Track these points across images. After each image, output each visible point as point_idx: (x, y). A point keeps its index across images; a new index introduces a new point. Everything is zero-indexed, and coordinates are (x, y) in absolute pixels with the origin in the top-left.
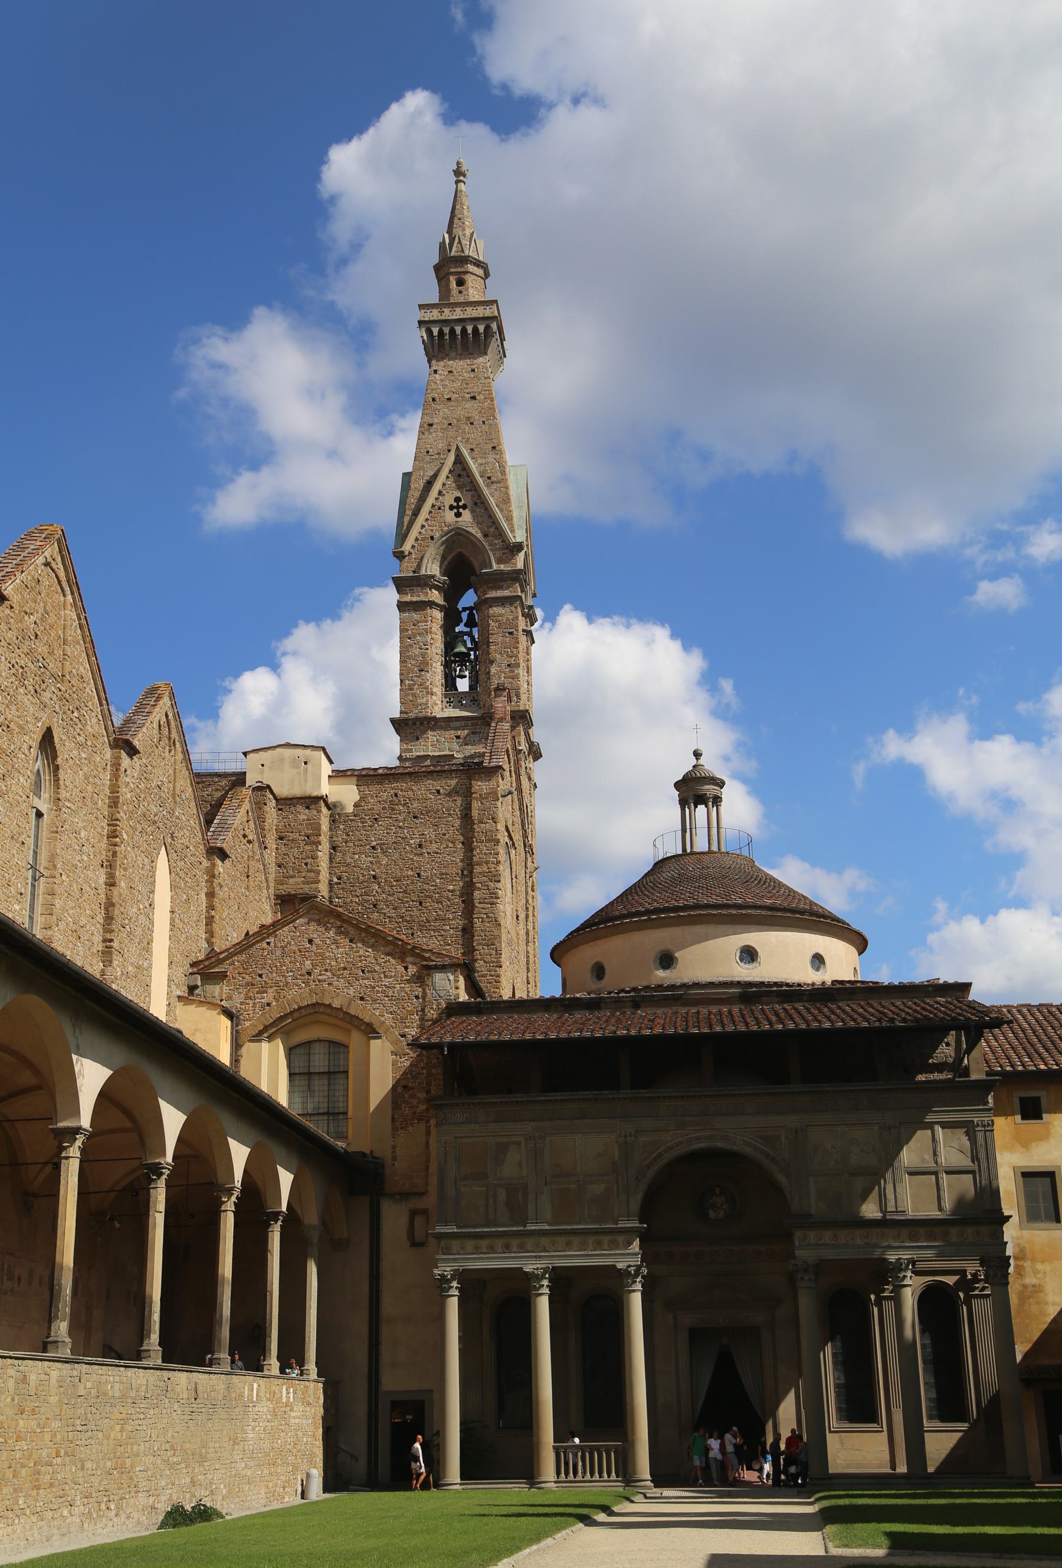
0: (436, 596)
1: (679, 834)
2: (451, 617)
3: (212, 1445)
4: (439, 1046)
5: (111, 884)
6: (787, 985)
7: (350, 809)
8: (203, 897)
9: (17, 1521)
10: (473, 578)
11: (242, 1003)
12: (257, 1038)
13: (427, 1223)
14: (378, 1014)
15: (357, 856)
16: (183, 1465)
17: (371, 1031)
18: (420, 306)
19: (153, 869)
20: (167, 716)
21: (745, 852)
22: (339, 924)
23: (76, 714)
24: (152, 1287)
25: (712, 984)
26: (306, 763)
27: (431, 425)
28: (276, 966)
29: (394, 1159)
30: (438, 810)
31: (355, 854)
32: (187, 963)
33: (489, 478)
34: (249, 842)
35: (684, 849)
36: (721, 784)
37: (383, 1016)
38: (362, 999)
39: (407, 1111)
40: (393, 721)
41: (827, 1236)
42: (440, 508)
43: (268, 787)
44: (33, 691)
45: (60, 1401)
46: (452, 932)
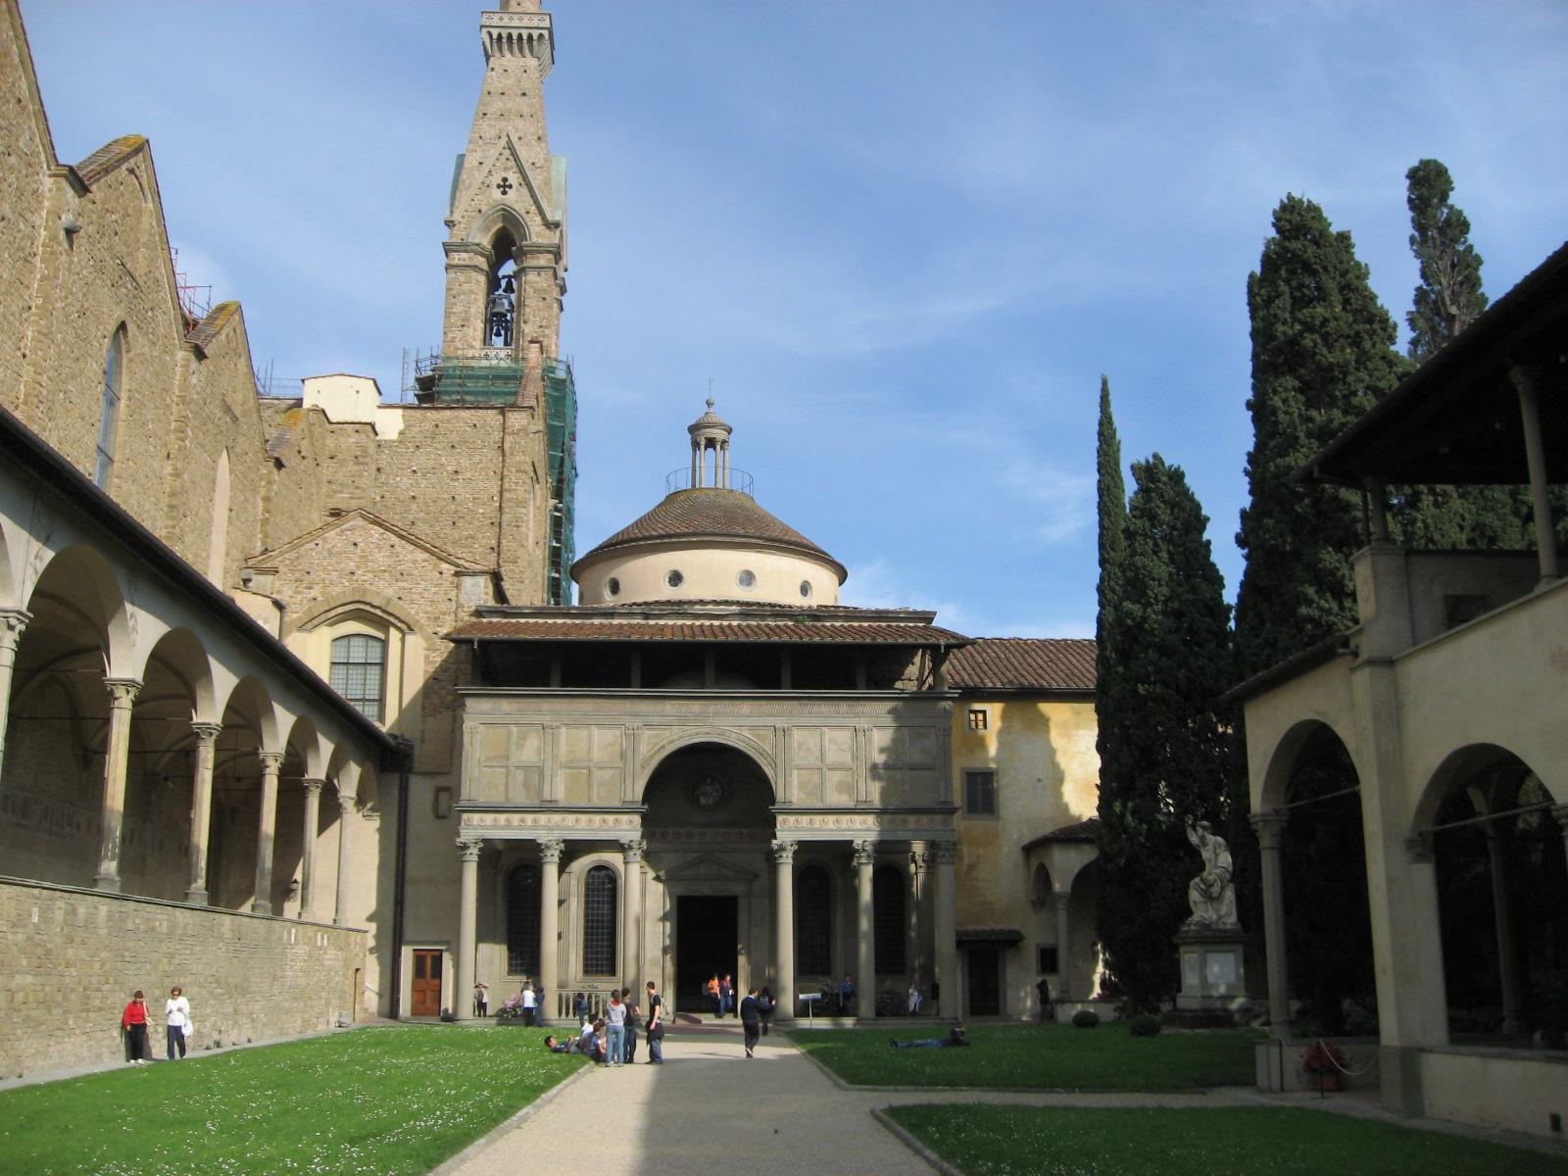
0: (482, 262)
1: (690, 470)
2: (493, 284)
3: (253, 979)
4: (470, 642)
6: (780, 606)
7: (394, 436)
8: (259, 499)
9: (67, 1040)
10: (514, 248)
11: (291, 597)
12: (301, 628)
13: (450, 798)
14: (413, 613)
15: (398, 479)
16: (227, 996)
19: (214, 469)
20: (235, 330)
21: (746, 491)
22: (382, 531)
23: (150, 314)
24: (199, 836)
25: (714, 602)
26: (358, 392)
27: (485, 114)
28: (323, 566)
29: (423, 741)
30: (473, 442)
31: (397, 476)
32: (241, 557)
33: (533, 164)
34: (304, 458)
35: (694, 485)
36: (730, 431)
37: (418, 614)
38: (400, 598)
41: (805, 819)
42: (488, 186)
43: (323, 411)
44: (110, 285)
45: (109, 934)
46: (480, 550)
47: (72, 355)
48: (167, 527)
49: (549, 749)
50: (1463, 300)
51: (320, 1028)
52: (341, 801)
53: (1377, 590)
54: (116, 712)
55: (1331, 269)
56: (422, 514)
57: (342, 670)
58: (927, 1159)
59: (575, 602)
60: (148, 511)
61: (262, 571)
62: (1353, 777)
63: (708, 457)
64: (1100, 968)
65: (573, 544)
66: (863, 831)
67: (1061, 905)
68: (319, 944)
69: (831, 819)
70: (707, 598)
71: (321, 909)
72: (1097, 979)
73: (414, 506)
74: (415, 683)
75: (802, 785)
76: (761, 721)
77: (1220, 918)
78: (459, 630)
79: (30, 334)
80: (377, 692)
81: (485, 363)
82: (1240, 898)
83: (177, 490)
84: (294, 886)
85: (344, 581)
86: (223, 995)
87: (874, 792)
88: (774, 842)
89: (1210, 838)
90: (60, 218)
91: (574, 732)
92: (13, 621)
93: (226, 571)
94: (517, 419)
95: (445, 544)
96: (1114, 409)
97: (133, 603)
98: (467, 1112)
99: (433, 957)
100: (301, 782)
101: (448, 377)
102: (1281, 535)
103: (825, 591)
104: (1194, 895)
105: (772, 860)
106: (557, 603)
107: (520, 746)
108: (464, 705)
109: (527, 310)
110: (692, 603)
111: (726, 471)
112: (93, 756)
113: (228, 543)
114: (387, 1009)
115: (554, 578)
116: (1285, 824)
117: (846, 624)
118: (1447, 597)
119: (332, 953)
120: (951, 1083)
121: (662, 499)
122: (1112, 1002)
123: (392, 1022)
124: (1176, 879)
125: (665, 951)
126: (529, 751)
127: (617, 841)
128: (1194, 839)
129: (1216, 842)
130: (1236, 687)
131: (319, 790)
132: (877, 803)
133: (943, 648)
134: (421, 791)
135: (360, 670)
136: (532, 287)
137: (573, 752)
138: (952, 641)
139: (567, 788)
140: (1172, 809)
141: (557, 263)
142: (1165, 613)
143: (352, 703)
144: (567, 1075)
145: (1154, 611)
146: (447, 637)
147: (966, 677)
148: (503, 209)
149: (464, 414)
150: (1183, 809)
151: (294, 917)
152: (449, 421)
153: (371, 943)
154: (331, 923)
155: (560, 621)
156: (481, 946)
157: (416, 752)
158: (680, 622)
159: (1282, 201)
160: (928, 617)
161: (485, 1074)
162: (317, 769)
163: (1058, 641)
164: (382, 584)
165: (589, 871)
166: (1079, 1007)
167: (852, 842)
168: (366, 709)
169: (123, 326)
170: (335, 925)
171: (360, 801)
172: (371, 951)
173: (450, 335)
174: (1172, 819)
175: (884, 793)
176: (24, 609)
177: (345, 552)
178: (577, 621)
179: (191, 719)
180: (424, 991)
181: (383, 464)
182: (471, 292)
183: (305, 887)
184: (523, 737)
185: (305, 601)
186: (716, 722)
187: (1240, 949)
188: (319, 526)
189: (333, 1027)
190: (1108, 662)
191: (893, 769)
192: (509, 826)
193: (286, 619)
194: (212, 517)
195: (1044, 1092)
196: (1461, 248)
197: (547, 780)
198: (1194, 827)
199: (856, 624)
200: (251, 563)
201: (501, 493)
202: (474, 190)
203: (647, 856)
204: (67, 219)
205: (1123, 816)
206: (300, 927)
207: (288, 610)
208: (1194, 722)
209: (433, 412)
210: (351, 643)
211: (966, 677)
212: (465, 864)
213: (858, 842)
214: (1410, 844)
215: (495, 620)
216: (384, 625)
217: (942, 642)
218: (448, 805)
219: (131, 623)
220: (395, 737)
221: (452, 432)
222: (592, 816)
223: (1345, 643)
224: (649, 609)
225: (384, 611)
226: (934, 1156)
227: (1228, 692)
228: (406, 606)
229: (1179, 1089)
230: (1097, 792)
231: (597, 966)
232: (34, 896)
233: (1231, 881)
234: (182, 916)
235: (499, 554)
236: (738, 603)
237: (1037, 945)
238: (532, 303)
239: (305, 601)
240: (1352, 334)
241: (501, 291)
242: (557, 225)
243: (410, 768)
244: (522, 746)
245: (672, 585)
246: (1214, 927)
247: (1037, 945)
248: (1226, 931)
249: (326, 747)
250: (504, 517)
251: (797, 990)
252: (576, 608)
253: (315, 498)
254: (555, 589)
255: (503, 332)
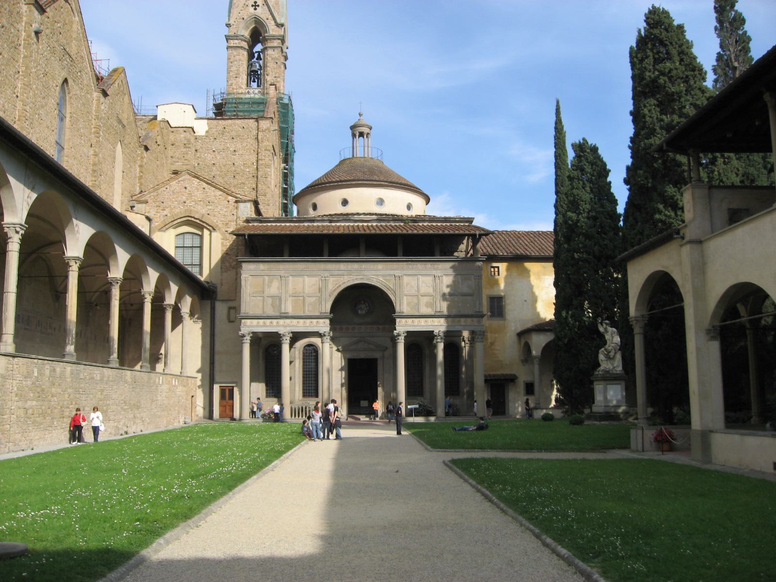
0: (245, 45)
1: (351, 149)
2: (251, 56)
3: (142, 401)
4: (244, 235)
6: (397, 215)
7: (203, 133)
9: (54, 432)
10: (261, 37)
11: (155, 215)
12: (160, 230)
13: (236, 312)
17: (212, 229)
19: (114, 152)
22: (198, 181)
23: (79, 74)
25: (364, 214)
29: (222, 284)
32: (129, 195)
34: (159, 145)
35: (353, 156)
39: (228, 264)
41: (410, 320)
43: (168, 121)
45: (72, 381)
47: (41, 96)
48: (92, 181)
49: (283, 287)
50: (741, 59)
51: (175, 424)
52: (182, 314)
53: (694, 206)
54: (71, 273)
55: (674, 43)
56: (218, 172)
57: (181, 250)
58: (470, 484)
59: (295, 214)
60: (83, 173)
61: (140, 202)
62: (681, 300)
63: (360, 141)
64: (555, 392)
65: (294, 186)
66: (439, 326)
67: (536, 362)
68: (174, 384)
69: (423, 320)
70: (361, 212)
71: (174, 367)
72: (553, 398)
73: (214, 168)
74: (217, 256)
75: (408, 304)
76: (388, 272)
77: (614, 368)
78: (238, 230)
79: (19, 85)
80: (198, 261)
81: (248, 96)
82: (624, 358)
83: (97, 162)
84: (161, 356)
85: (181, 206)
86: (128, 409)
87: (443, 307)
88: (395, 331)
89: (610, 329)
90: (31, 26)
91: (296, 279)
92: (18, 229)
93: (122, 203)
94: (264, 124)
95: (230, 187)
96: (563, 116)
97: (76, 219)
98: (248, 463)
99: (229, 389)
100: (162, 306)
101: (229, 103)
102: (646, 178)
103: (419, 208)
104: (601, 357)
105: (394, 340)
106: (286, 215)
107: (269, 286)
108: (242, 266)
109: (268, 69)
110: (353, 214)
111: (369, 148)
112: (60, 295)
113: (122, 189)
114: (207, 415)
115: (284, 203)
116: (646, 322)
117: (429, 224)
118: (729, 209)
119: (180, 388)
120: (482, 448)
121: (338, 163)
122: (561, 409)
123: (210, 421)
124: (593, 349)
125: (342, 385)
126: (274, 289)
127: (318, 332)
128: (601, 329)
129: (612, 331)
130: (623, 255)
131: (171, 309)
132: (445, 312)
133: (478, 236)
134: (221, 309)
135: (190, 250)
136: (270, 57)
137: (295, 289)
138: (482, 232)
139: (293, 307)
140: (591, 315)
141: (283, 45)
142: (588, 218)
143: (186, 267)
144: (295, 445)
145: (583, 217)
146: (232, 233)
147: (489, 250)
148: (255, 18)
149: (238, 122)
150: (596, 315)
151: (161, 371)
152: (231, 126)
153: (199, 383)
154: (179, 374)
155: (288, 224)
156: (252, 384)
157: (218, 290)
158: (347, 224)
159: (649, 9)
160: (470, 220)
161: (255, 446)
162: (170, 299)
163: (535, 232)
164: (199, 207)
165: (305, 347)
166: (544, 411)
167: (433, 331)
168: (193, 269)
169: (66, 81)
170: (181, 375)
171: (192, 315)
172: (199, 387)
173: (230, 82)
174: (591, 320)
175: (449, 307)
176: (23, 223)
177: (181, 192)
178: (296, 224)
179: (108, 276)
180: (225, 406)
181: (198, 148)
182: (240, 60)
183: (166, 356)
184: (271, 282)
185: (162, 217)
186: (366, 273)
187: (623, 383)
188: (167, 179)
189: (182, 424)
190: (559, 242)
191: (454, 295)
192: (265, 325)
193: (153, 225)
194: (114, 176)
195: (527, 452)
196: (741, 32)
197: (283, 302)
198: (601, 323)
199: (434, 224)
200: (134, 198)
201: (257, 161)
202: (240, 7)
203: (333, 339)
204: (35, 26)
205: (566, 318)
206: (164, 376)
207: (153, 221)
208: (602, 272)
209: (223, 121)
210: (185, 237)
211: (489, 250)
212: (244, 344)
213: (436, 332)
214: (708, 332)
215: (255, 224)
216: (201, 227)
217: (477, 233)
218: (235, 316)
219: (76, 229)
220: (208, 283)
221: (232, 131)
222: (305, 320)
223: (678, 233)
224: (332, 218)
225: (201, 221)
226: (474, 483)
227: (619, 257)
228: (212, 218)
229: (593, 450)
230: (554, 307)
231: (309, 393)
232: (34, 363)
233: (620, 350)
234: (106, 371)
235: (257, 191)
236: (376, 214)
237: (524, 381)
238: (271, 66)
239: (162, 217)
240: (684, 76)
242: (282, 25)
243: (216, 298)
244: (270, 286)
245: (343, 206)
246: (611, 372)
247: (524, 381)
248: (617, 374)
249: (174, 288)
250: (260, 173)
251: (407, 404)
252: (295, 218)
253: (165, 165)
254: (285, 208)
255: (256, 80)
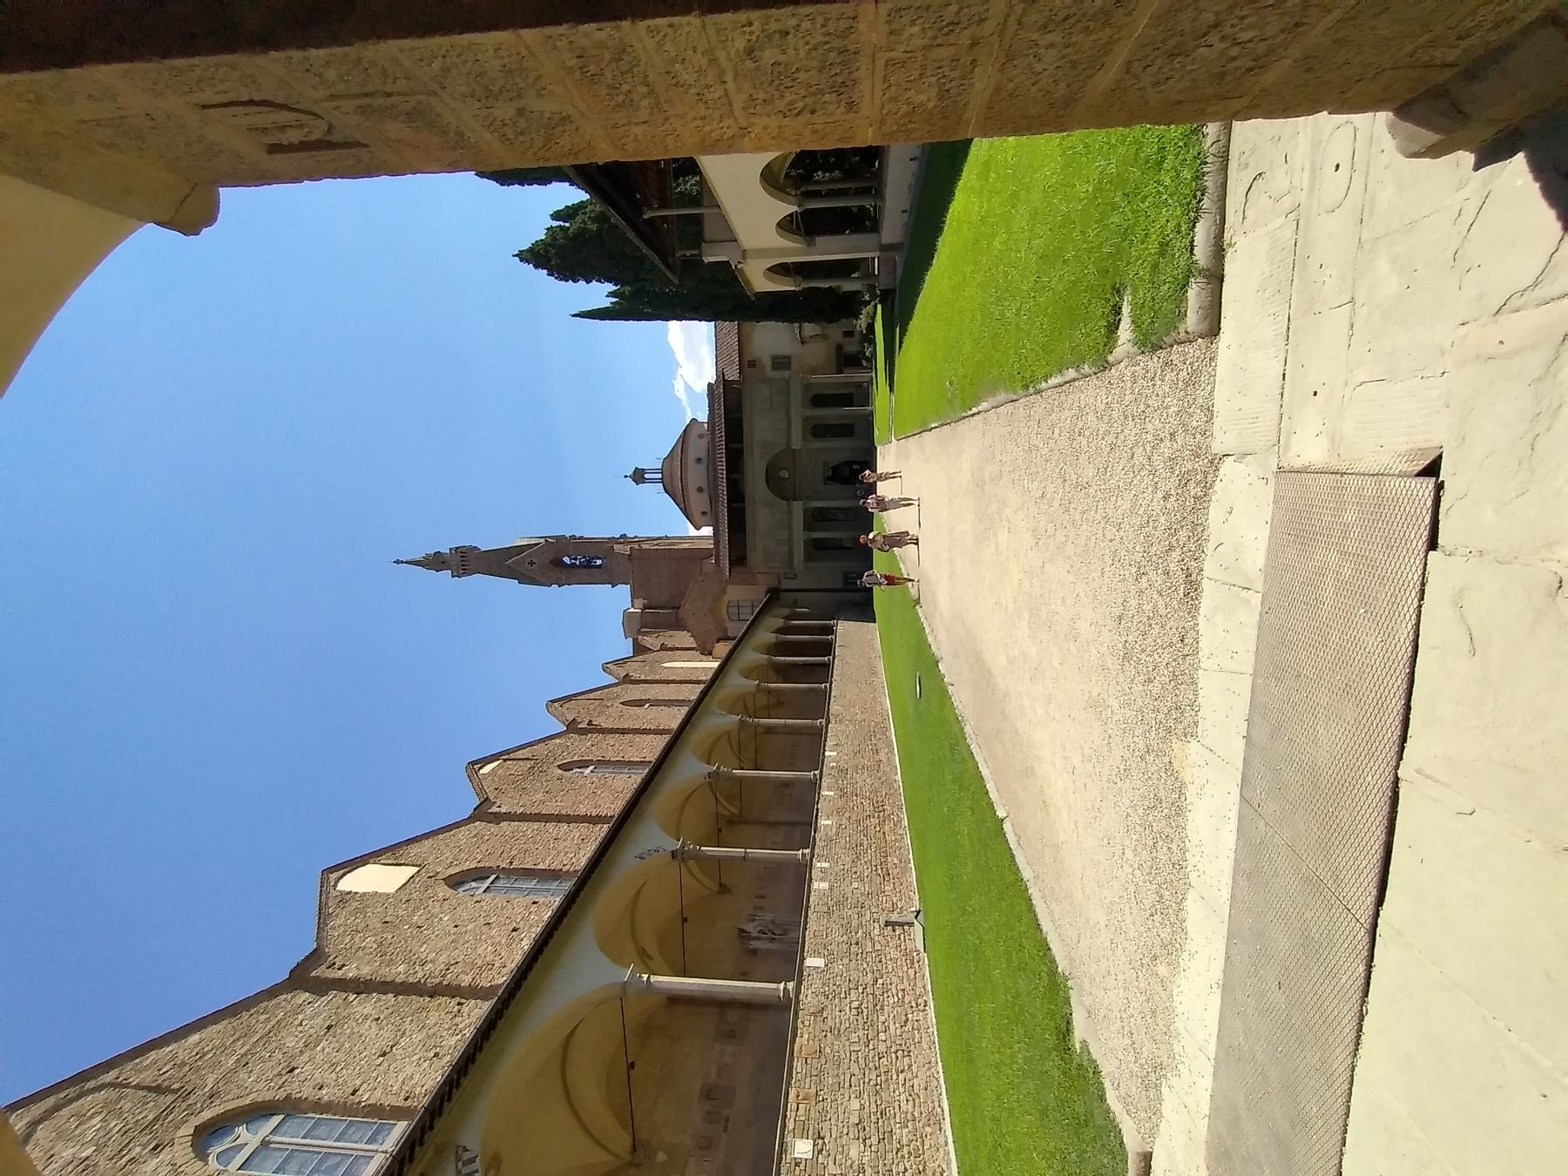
5: (673, 682)
12: (727, 632)
18: (453, 577)
19: (666, 668)
40: (613, 587)
241: (578, 563)
